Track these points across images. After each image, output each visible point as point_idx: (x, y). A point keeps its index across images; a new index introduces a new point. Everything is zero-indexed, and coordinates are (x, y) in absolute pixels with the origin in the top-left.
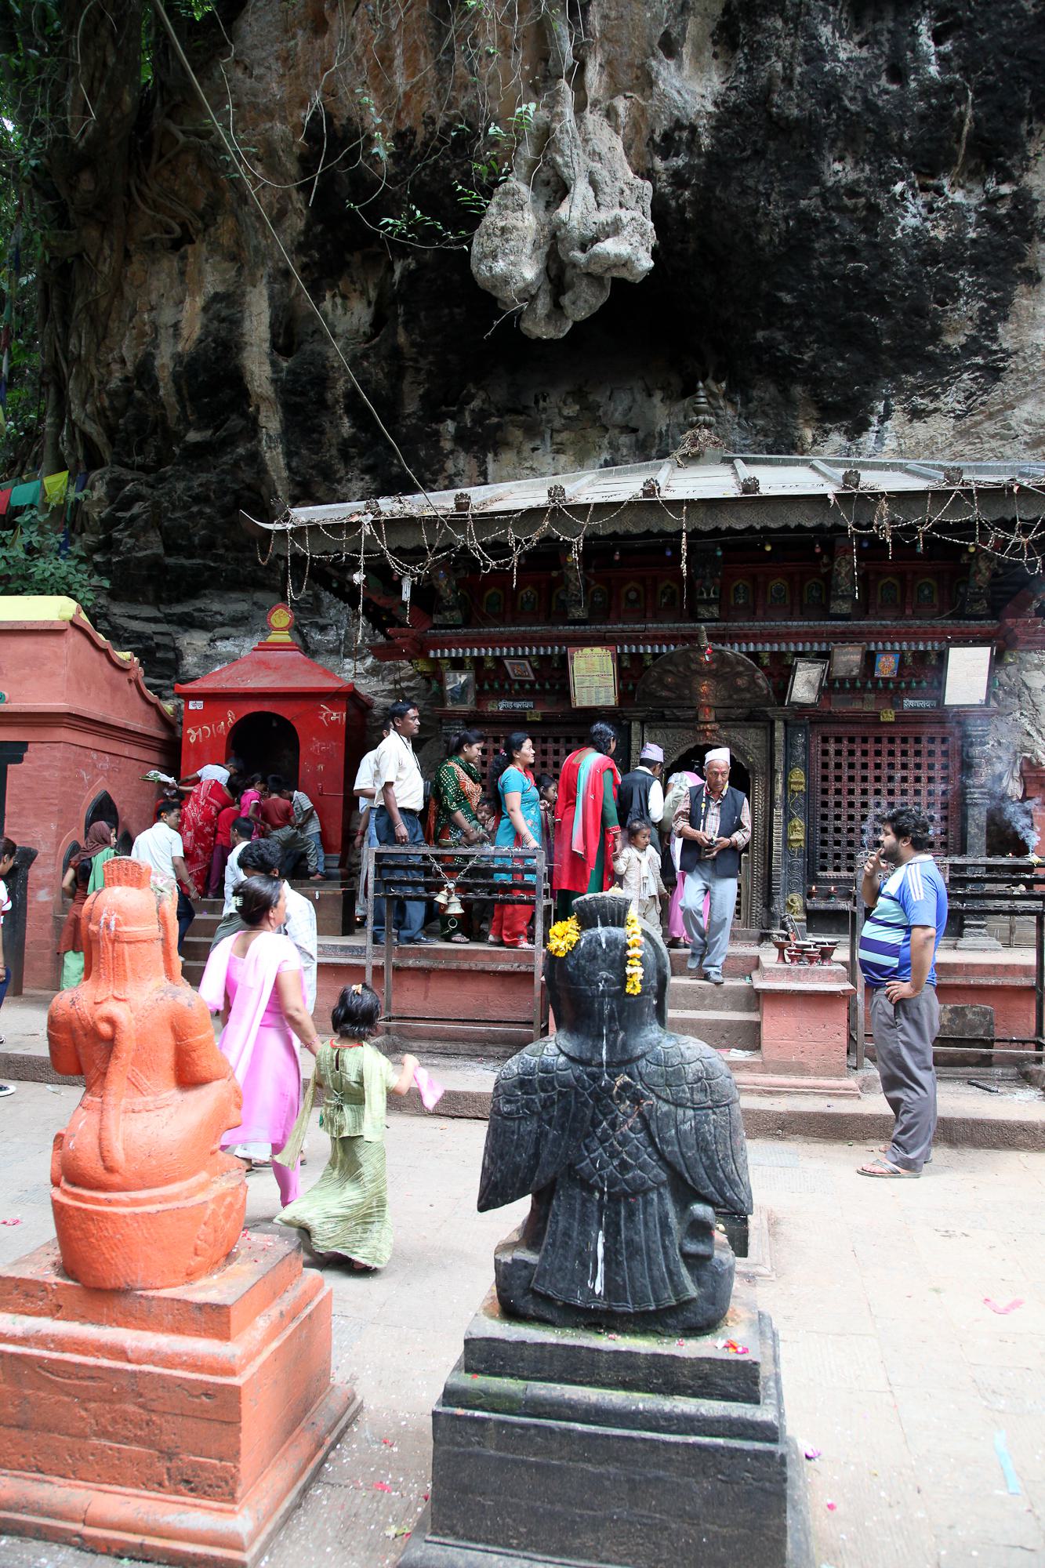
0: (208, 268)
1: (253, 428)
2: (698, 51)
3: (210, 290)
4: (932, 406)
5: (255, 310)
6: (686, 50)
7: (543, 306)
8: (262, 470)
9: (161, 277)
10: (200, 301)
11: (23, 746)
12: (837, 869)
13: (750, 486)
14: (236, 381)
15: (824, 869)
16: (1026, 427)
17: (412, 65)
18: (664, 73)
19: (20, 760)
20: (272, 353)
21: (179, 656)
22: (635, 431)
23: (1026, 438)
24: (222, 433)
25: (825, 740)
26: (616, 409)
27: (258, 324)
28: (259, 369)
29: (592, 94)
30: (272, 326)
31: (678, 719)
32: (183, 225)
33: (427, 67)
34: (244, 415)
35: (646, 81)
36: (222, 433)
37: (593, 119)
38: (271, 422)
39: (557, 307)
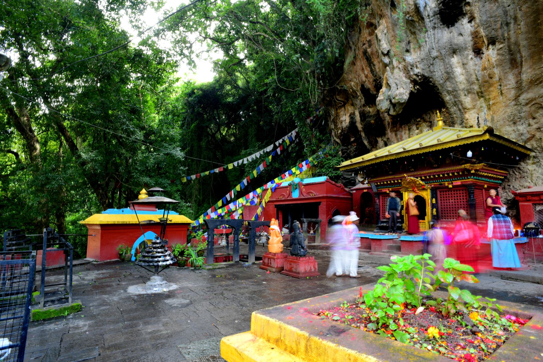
2: (414, 49)
6: (412, 50)
9: (342, 112)
11: (320, 202)
13: (404, 149)
17: (366, 69)
18: (407, 58)
21: (356, 181)
25: (440, 192)
26: (427, 118)
27: (358, 118)
28: (359, 126)
29: (395, 66)
30: (360, 117)
33: (369, 69)
35: (404, 60)
37: (396, 71)
38: (363, 134)
39: (394, 111)
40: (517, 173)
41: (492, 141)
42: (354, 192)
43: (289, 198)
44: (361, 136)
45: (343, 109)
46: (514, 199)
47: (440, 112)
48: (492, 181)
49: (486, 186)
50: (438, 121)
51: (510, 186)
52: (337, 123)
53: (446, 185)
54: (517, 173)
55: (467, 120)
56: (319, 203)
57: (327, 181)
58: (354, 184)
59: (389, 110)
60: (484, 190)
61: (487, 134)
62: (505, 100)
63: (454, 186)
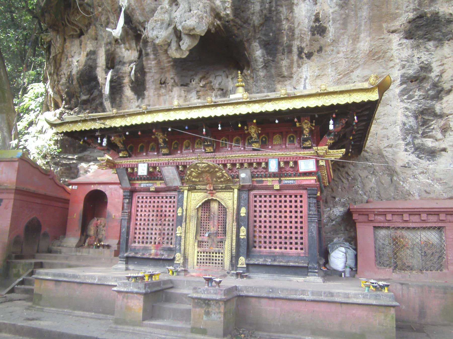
0: (88, 42)
3: (88, 50)
4: (323, 74)
5: (101, 55)
7: (174, 45)
10: (85, 53)
16: (357, 79)
20: (106, 69)
22: (222, 90)
24: (92, 97)
27: (102, 60)
31: (201, 189)
32: (81, 30)
34: (98, 90)
36: (92, 97)
40: (345, 181)
42: (75, 187)
44: (101, 95)
45: (77, 42)
50: (238, 86)
52: (60, 66)
53: (269, 184)
54: (345, 181)
59: (169, 45)
61: (377, 91)
63: (282, 188)
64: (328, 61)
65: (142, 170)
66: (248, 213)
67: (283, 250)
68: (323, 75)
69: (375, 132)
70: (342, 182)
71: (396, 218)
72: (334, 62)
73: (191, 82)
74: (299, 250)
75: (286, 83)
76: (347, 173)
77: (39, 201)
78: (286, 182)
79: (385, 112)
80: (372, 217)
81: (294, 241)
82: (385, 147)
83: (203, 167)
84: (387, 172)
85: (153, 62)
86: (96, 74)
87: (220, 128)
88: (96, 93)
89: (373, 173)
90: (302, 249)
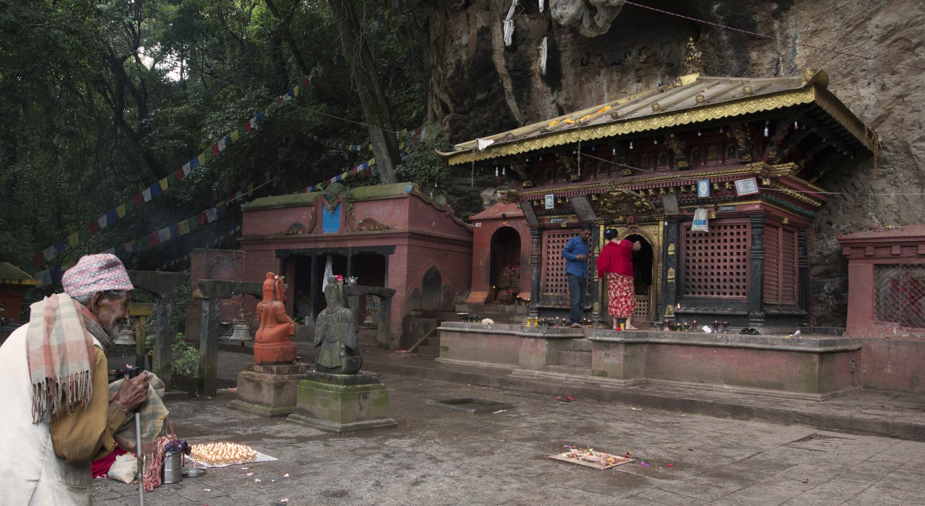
0: (478, 15)
1: (502, 90)
3: (479, 26)
4: (821, 27)
5: (496, 34)
7: (586, 23)
8: (508, 109)
11: (394, 247)
12: (725, 294)
14: (492, 67)
15: (687, 293)
16: (876, 30)
19: (393, 253)
20: (504, 54)
22: (672, 65)
23: (875, 37)
34: (498, 84)
39: (593, 25)
41: (819, 108)
43: (312, 235)
45: (463, 16)
46: (840, 253)
47: (695, 41)
48: (799, 208)
49: (786, 221)
51: (831, 224)
52: (444, 52)
54: (849, 198)
55: (754, 65)
56: (391, 249)
57: (412, 194)
58: (479, 208)
59: (581, 21)
60: (781, 230)
62: (838, 25)
64: (828, 6)
65: (549, 202)
66: (678, 251)
67: (722, 296)
68: (822, 30)
69: (899, 118)
70: (846, 199)
71: (907, 252)
72: (839, 6)
73: (626, 57)
74: (741, 296)
75: (765, 48)
76: (853, 185)
77: (436, 246)
78: (724, 209)
79: (918, 84)
80: (870, 251)
81: (735, 284)
82: (915, 142)
83: (617, 196)
84: (917, 181)
85: (569, 36)
86: (492, 61)
87: (631, 147)
88: (495, 88)
89: (895, 184)
90: (744, 294)
